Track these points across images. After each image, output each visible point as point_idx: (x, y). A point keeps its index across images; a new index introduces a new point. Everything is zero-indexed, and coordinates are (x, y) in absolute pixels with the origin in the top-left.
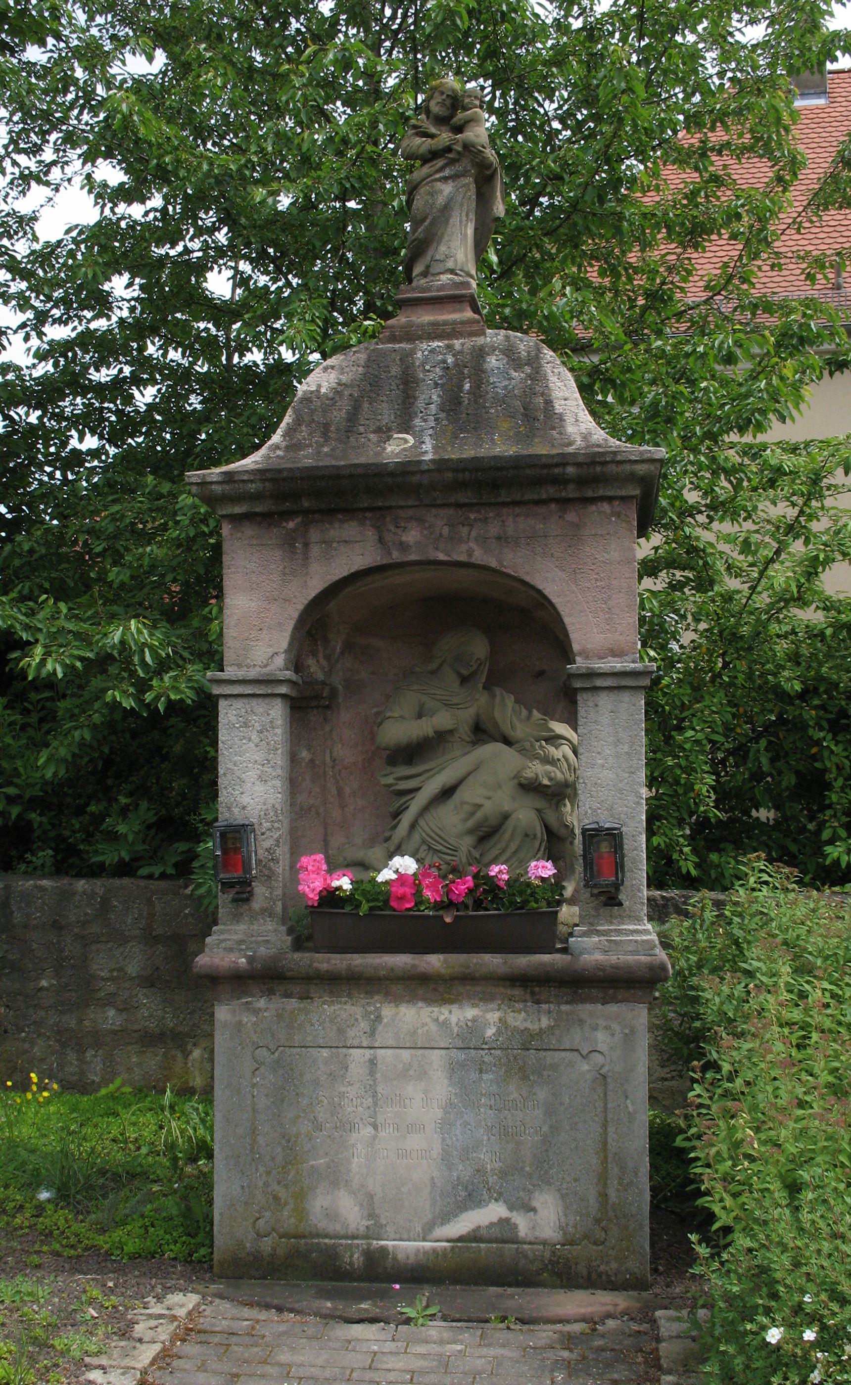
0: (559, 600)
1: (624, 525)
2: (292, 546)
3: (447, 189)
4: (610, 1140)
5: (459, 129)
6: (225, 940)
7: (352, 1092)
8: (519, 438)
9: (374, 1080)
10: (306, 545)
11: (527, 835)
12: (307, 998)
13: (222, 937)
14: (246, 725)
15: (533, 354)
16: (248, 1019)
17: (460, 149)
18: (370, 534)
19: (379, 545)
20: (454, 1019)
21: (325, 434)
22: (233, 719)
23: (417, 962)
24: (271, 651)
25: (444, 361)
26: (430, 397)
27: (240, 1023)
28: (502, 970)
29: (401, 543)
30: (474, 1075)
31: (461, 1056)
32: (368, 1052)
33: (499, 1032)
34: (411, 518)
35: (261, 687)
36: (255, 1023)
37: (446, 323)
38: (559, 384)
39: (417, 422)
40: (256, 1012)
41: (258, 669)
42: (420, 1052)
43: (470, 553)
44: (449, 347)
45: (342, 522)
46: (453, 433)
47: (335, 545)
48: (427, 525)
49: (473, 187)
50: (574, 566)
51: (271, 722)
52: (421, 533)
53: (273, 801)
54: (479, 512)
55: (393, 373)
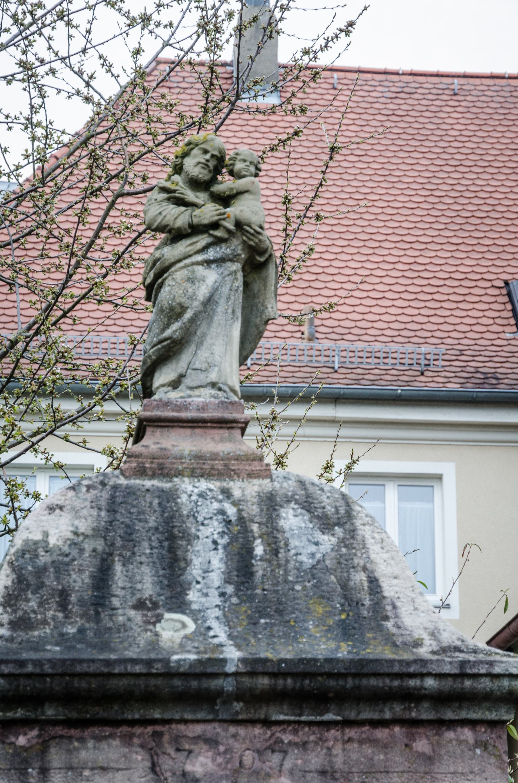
1: (493, 760)
2: (23, 772)
3: (211, 276)
5: (225, 200)
15: (342, 511)
17: (231, 227)
18: (140, 758)
19: (151, 776)
25: (222, 512)
26: (208, 563)
37: (214, 457)
38: (385, 556)
39: (192, 596)
44: (227, 493)
45: (98, 739)
46: (249, 617)
47: (86, 773)
48: (222, 748)
49: (240, 275)
52: (214, 760)
54: (295, 732)
55: (152, 523)
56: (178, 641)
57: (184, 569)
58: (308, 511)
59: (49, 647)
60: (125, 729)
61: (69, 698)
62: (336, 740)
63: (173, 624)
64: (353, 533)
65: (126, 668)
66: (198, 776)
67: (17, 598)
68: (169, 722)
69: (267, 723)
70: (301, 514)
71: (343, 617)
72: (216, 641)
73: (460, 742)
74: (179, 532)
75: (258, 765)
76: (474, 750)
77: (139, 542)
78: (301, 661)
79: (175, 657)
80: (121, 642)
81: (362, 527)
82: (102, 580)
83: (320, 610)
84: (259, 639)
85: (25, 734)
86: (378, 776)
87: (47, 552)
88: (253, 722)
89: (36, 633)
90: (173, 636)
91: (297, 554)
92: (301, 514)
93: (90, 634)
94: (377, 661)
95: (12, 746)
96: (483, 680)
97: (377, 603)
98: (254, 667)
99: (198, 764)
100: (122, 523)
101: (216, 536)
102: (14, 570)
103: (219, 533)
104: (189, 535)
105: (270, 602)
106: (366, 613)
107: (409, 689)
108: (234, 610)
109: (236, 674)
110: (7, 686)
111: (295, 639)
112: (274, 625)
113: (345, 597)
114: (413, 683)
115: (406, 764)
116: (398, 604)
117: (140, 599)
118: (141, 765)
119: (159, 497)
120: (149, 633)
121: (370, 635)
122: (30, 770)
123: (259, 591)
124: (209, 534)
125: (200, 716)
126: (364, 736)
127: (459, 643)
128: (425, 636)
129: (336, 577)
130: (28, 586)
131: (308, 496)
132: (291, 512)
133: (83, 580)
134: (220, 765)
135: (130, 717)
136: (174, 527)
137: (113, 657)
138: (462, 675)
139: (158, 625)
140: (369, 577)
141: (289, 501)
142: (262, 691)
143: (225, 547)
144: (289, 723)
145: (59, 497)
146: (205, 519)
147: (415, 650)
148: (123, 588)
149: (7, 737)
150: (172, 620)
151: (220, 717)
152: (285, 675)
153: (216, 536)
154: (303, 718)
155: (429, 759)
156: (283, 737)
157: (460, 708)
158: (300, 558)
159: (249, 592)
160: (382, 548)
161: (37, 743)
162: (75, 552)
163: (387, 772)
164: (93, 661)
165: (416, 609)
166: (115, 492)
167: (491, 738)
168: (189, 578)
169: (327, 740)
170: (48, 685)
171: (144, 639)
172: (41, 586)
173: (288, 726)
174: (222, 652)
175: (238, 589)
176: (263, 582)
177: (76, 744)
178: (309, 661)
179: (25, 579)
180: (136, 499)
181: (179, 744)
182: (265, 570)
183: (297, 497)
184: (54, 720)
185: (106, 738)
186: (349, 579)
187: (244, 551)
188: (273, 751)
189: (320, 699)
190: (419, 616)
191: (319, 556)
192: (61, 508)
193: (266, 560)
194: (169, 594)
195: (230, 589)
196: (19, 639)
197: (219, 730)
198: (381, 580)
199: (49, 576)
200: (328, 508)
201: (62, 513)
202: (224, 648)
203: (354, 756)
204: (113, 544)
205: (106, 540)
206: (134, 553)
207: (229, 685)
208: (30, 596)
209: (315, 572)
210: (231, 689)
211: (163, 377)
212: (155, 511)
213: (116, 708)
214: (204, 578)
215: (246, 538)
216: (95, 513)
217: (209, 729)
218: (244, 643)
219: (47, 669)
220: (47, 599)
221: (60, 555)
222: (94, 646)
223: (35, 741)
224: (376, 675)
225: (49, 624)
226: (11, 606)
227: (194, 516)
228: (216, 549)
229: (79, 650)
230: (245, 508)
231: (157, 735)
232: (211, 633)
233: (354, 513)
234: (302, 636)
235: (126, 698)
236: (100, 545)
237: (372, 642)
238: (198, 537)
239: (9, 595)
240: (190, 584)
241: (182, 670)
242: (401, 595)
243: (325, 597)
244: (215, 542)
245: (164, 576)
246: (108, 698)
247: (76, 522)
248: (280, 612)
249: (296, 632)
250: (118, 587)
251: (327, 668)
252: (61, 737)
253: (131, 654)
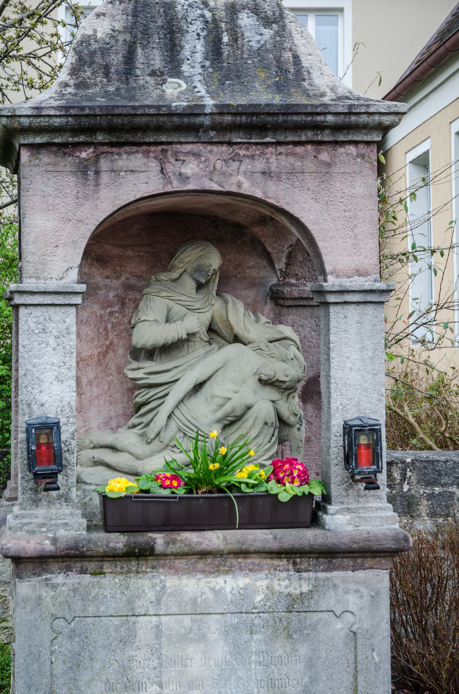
0: (315, 227)
2: (85, 173)
4: (359, 688)
6: (28, 524)
7: (140, 655)
8: (279, 87)
9: (160, 643)
10: (97, 173)
11: (266, 424)
12: (101, 573)
13: (24, 521)
14: (44, 331)
15: (277, 14)
16: (47, 594)
18: (154, 165)
19: (161, 175)
20: (228, 589)
21: (107, 74)
22: (33, 326)
23: (201, 540)
24: (66, 265)
25: (203, 16)
26: (194, 47)
27: (40, 598)
28: (275, 546)
29: (180, 174)
30: (246, 636)
31: (234, 619)
32: (154, 619)
33: (267, 598)
34: (189, 152)
35: (56, 298)
36: (53, 597)
38: (304, 41)
39: (185, 68)
40: (54, 587)
41: (54, 281)
42: (199, 617)
43: (239, 185)
46: (219, 80)
47: (122, 174)
48: (203, 159)
50: (326, 199)
51: (67, 329)
52: (198, 166)
53: (68, 399)
54: (247, 149)
55: (160, 24)
56: (176, 95)
57: (180, 52)
58: (256, 14)
59: (98, 99)
60: (145, 148)
61: (111, 129)
62: (272, 153)
63: (173, 84)
64: (284, 27)
65: (145, 111)
66: (189, 175)
67: (79, 70)
68: (171, 143)
69: (230, 144)
70: (252, 16)
71: (277, 79)
72: (199, 94)
73: (348, 154)
74: (177, 28)
75: (225, 168)
76: (356, 159)
77: (152, 35)
78: (251, 105)
79: (174, 104)
80: (142, 96)
81: (289, 24)
82: (130, 58)
83: (263, 75)
84: (225, 93)
85: (86, 151)
86: (297, 175)
87: (96, 42)
88: (221, 143)
89: (91, 91)
90: (173, 92)
91: (249, 41)
92: (252, 16)
93: (123, 91)
94: (297, 105)
95: (78, 158)
96: (362, 116)
97: (298, 71)
98: (223, 109)
99: (188, 168)
100: (141, 23)
101: (199, 31)
102: (76, 53)
103: (200, 29)
104: (182, 30)
105: (232, 71)
106: (291, 76)
107: (317, 122)
108: (210, 76)
109: (211, 114)
110: (74, 123)
111: (248, 93)
112: (234, 84)
113: (278, 67)
114: (319, 118)
115: (315, 167)
116: (311, 71)
117: (153, 70)
118: (155, 169)
119: (163, 7)
120: (158, 90)
121: (294, 90)
122: (89, 172)
123: (225, 64)
124: (195, 29)
125: (190, 140)
126: (289, 151)
127: (348, 94)
128: (328, 90)
129: (273, 55)
130: (85, 62)
131: (256, 5)
132: (245, 15)
133: (118, 59)
134: (202, 169)
135: (148, 141)
136: (173, 25)
137: (137, 104)
138: (350, 113)
139: (164, 85)
140: (293, 54)
141: (244, 8)
142: (227, 124)
143: (205, 38)
144: (244, 143)
145: (102, 8)
146: (192, 20)
147: (321, 99)
148: (143, 63)
149: (75, 153)
150: (172, 82)
151: (202, 140)
152: (241, 114)
153: (199, 31)
154: (252, 141)
155: (329, 165)
156: (240, 152)
157: (348, 133)
158: (251, 43)
159: (219, 65)
160: (302, 37)
161: (93, 156)
162: (113, 42)
163: (303, 173)
164: (125, 107)
165: (322, 74)
166: (137, 4)
167: (367, 152)
168: (183, 57)
169: (266, 154)
170: (98, 121)
171: (156, 93)
172: (93, 62)
173: (243, 145)
174: (203, 101)
175: (212, 63)
176: (228, 59)
177: (116, 157)
178: (256, 105)
179: (83, 59)
180: (150, 8)
181: (177, 156)
182: (229, 51)
183: (249, 6)
184: (102, 143)
185: (133, 153)
186: (281, 56)
187: (216, 40)
188: (234, 161)
189: (263, 129)
190: (324, 79)
191: (262, 42)
192: (104, 15)
193: (230, 45)
194: (170, 67)
195: (208, 63)
196: (81, 95)
197: (201, 148)
198: (301, 56)
199: (97, 57)
200: (269, 12)
201: (105, 18)
202: (204, 99)
203: (283, 163)
204: (136, 37)
205: (132, 34)
206: (149, 42)
207: (207, 121)
208: (87, 69)
209: (260, 52)
210: (208, 123)
212: (161, 16)
213: (139, 135)
214: (191, 57)
215: (217, 31)
216: (124, 17)
217: (195, 148)
218: (216, 96)
219: (98, 112)
220: (97, 71)
221: (104, 44)
222: (125, 98)
223: (92, 155)
224: (296, 114)
225: (98, 85)
226: (75, 75)
227: (185, 18)
228: (199, 39)
229: (117, 100)
230: (217, 13)
231: (164, 151)
232: (196, 90)
233: (285, 15)
234: (252, 91)
235: (145, 129)
236: (128, 37)
237: (295, 94)
238: (188, 32)
239: (74, 68)
240: (183, 60)
241: (178, 112)
242: (312, 66)
243: (266, 67)
244: (198, 35)
245: (167, 56)
246: (134, 129)
247: (114, 24)
248: (238, 77)
249: (248, 89)
250: (139, 63)
251: (267, 110)
252: (107, 152)
253: (147, 103)
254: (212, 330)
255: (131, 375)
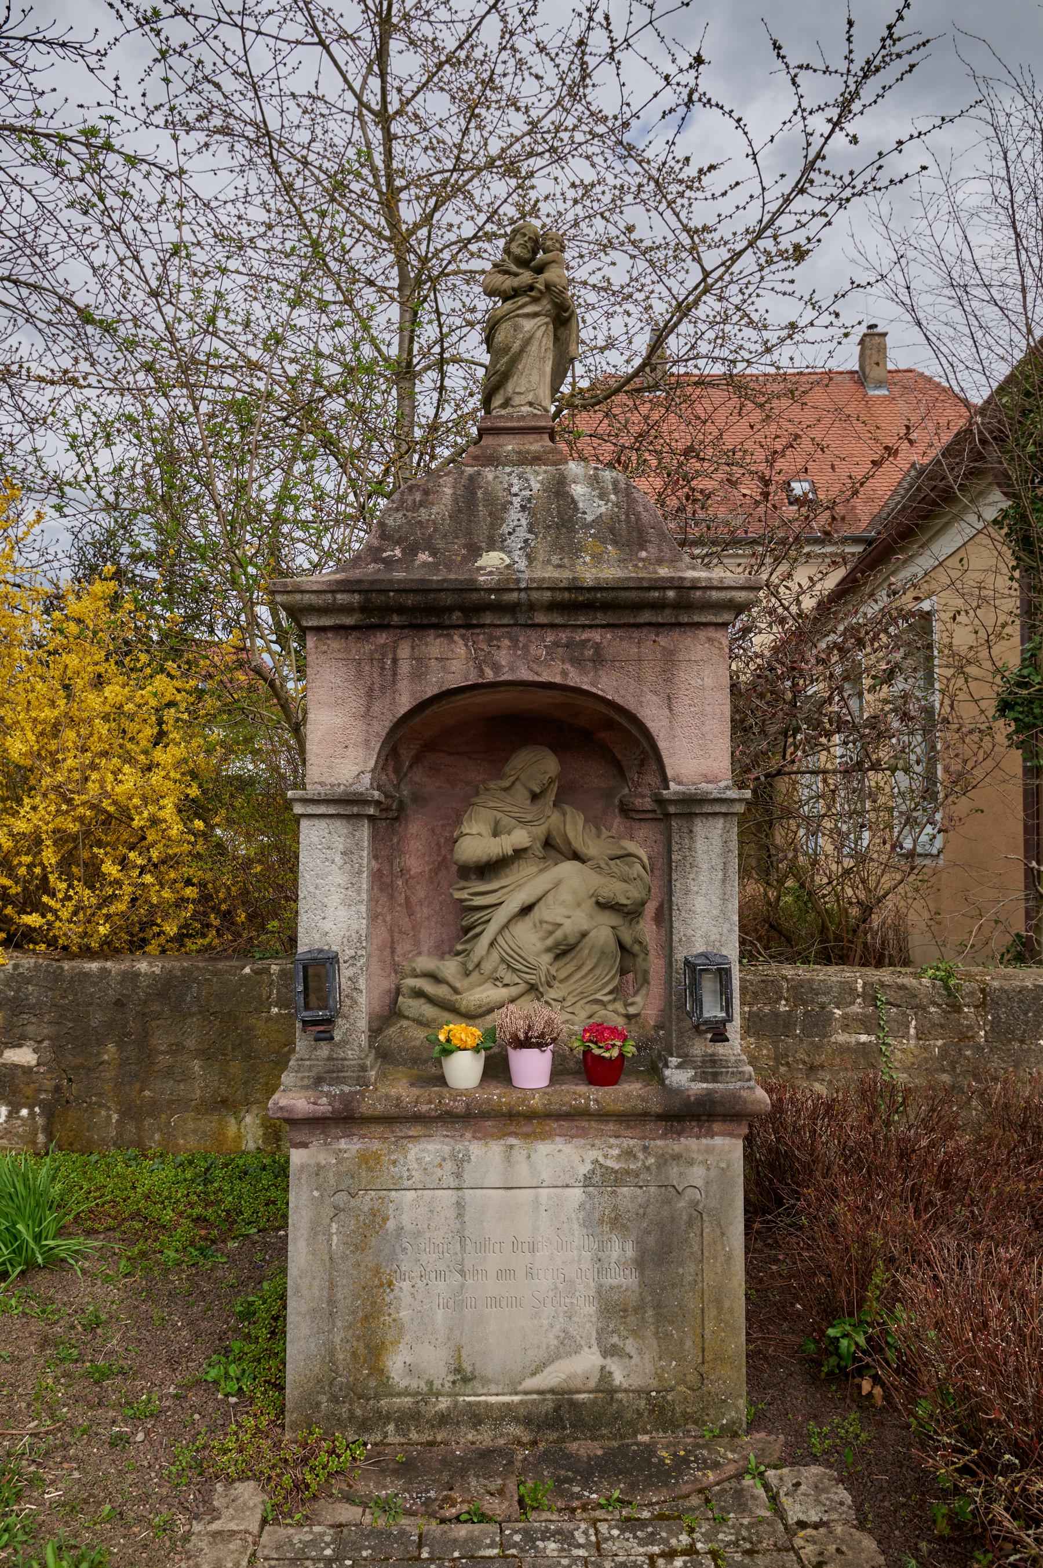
3: (528, 325)
5: (539, 270)
211: (497, 401)
254: (548, 843)
255: (457, 895)
